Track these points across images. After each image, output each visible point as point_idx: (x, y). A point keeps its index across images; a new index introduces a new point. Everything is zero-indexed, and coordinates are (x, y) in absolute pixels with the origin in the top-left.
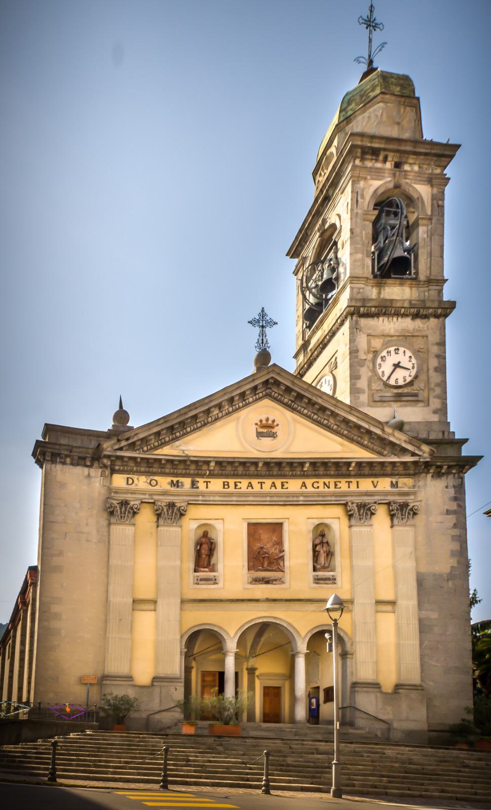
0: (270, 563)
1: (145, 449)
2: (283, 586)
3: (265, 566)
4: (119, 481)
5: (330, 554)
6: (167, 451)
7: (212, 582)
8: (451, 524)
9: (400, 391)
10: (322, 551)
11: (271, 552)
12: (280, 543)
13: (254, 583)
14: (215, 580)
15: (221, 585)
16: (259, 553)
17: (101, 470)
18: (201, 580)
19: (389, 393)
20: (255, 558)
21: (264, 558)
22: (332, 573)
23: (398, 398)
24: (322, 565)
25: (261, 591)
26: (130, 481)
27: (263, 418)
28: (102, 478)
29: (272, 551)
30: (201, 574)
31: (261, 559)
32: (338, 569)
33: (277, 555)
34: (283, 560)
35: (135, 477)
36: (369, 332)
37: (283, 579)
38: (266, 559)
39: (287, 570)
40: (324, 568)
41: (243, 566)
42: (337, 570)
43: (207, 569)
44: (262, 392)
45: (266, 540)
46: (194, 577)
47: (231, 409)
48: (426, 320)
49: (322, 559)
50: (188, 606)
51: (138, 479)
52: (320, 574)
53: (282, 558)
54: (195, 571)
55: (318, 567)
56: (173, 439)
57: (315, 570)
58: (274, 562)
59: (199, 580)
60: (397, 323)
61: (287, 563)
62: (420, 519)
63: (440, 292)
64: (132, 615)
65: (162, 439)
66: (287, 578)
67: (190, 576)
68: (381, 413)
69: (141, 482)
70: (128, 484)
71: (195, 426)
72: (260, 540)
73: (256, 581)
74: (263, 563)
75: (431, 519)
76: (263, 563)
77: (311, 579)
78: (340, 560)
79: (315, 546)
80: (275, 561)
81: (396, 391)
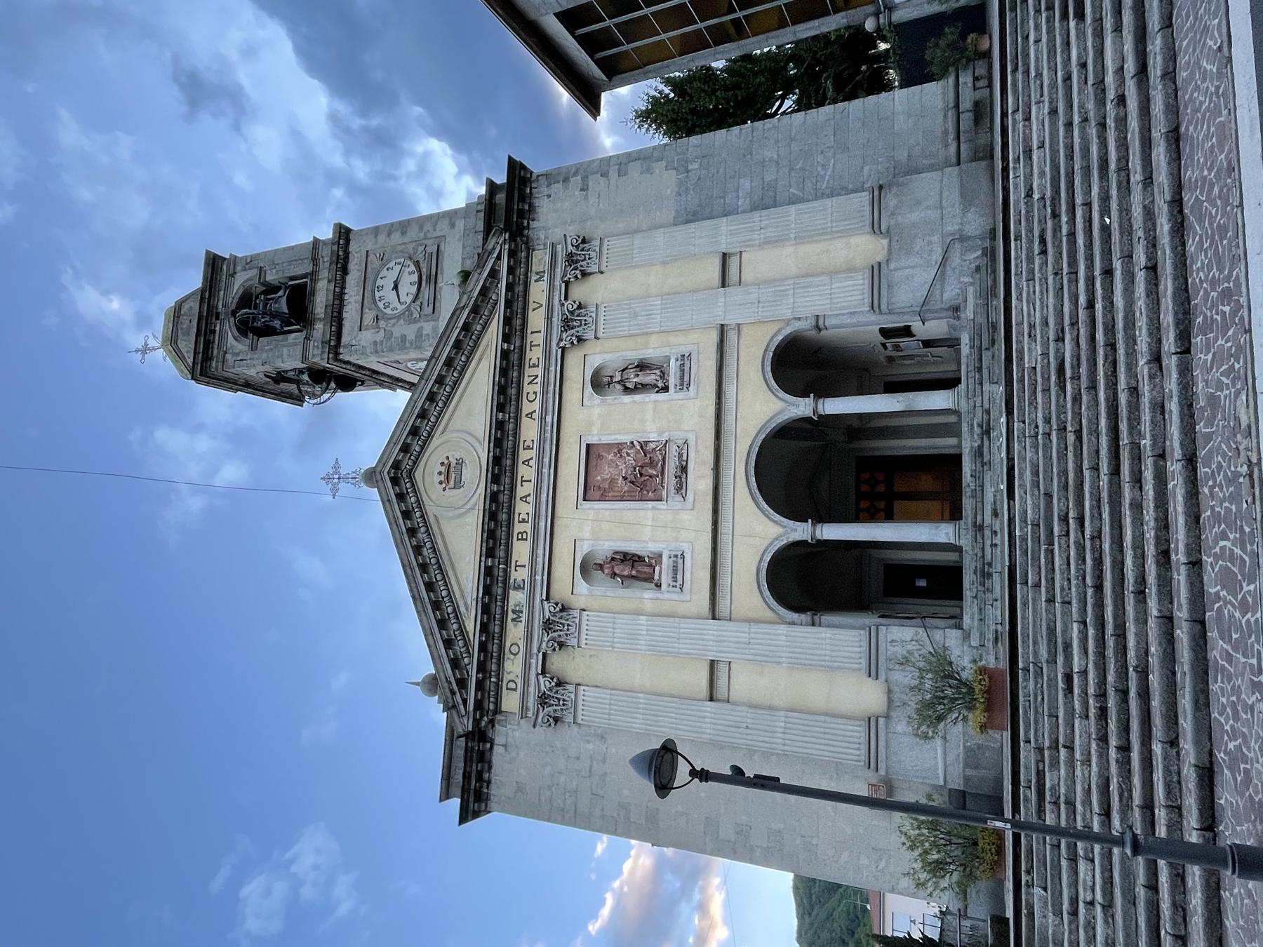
0: (652, 463)
1: (466, 660)
2: (692, 443)
3: (655, 473)
4: (510, 702)
5: (642, 366)
6: (471, 625)
7: (680, 561)
8: (602, 180)
9: (424, 278)
10: (633, 379)
11: (633, 462)
12: (619, 448)
13: (684, 491)
14: (676, 556)
15: (686, 547)
16: (632, 482)
17: (497, 726)
18: (675, 579)
19: (426, 293)
20: (641, 489)
21: (641, 475)
22: (672, 361)
23: (433, 279)
24: (658, 378)
25: (700, 481)
26: (512, 685)
27: (438, 478)
28: (508, 726)
29: (630, 460)
30: (666, 579)
31: (643, 479)
32: (666, 351)
33: (638, 452)
34: (646, 442)
35: (506, 678)
36: (356, 329)
37: (680, 442)
38: (643, 472)
39: (665, 437)
40: (663, 375)
41: (654, 508)
42: (668, 354)
43: (657, 569)
44: (406, 484)
45: (612, 470)
46: (668, 592)
47: (423, 530)
48: (350, 255)
49: (650, 378)
50: (723, 606)
51: (509, 673)
52: (673, 380)
53: (643, 445)
54: (659, 586)
55: (660, 384)
56: (456, 617)
57: (665, 389)
58: (650, 458)
59: (675, 584)
60: (351, 294)
61: (653, 437)
62: (595, 230)
63: (325, 243)
64: (736, 704)
65: (455, 635)
66: (678, 436)
67: (667, 598)
68: (450, 297)
69: (513, 667)
70: (515, 690)
71: (440, 583)
72: (612, 481)
73: (681, 487)
74: (651, 477)
75: (593, 212)
76: (651, 477)
77: (681, 395)
78: (651, 351)
79: (627, 390)
80: (648, 456)
81: (424, 283)
